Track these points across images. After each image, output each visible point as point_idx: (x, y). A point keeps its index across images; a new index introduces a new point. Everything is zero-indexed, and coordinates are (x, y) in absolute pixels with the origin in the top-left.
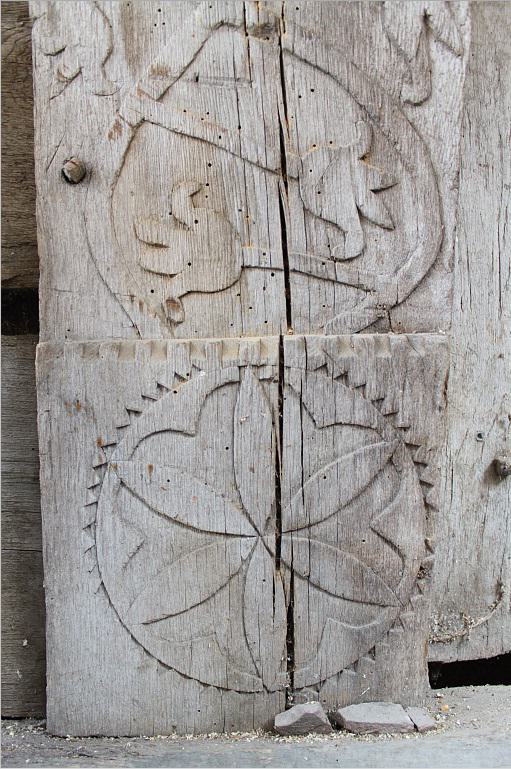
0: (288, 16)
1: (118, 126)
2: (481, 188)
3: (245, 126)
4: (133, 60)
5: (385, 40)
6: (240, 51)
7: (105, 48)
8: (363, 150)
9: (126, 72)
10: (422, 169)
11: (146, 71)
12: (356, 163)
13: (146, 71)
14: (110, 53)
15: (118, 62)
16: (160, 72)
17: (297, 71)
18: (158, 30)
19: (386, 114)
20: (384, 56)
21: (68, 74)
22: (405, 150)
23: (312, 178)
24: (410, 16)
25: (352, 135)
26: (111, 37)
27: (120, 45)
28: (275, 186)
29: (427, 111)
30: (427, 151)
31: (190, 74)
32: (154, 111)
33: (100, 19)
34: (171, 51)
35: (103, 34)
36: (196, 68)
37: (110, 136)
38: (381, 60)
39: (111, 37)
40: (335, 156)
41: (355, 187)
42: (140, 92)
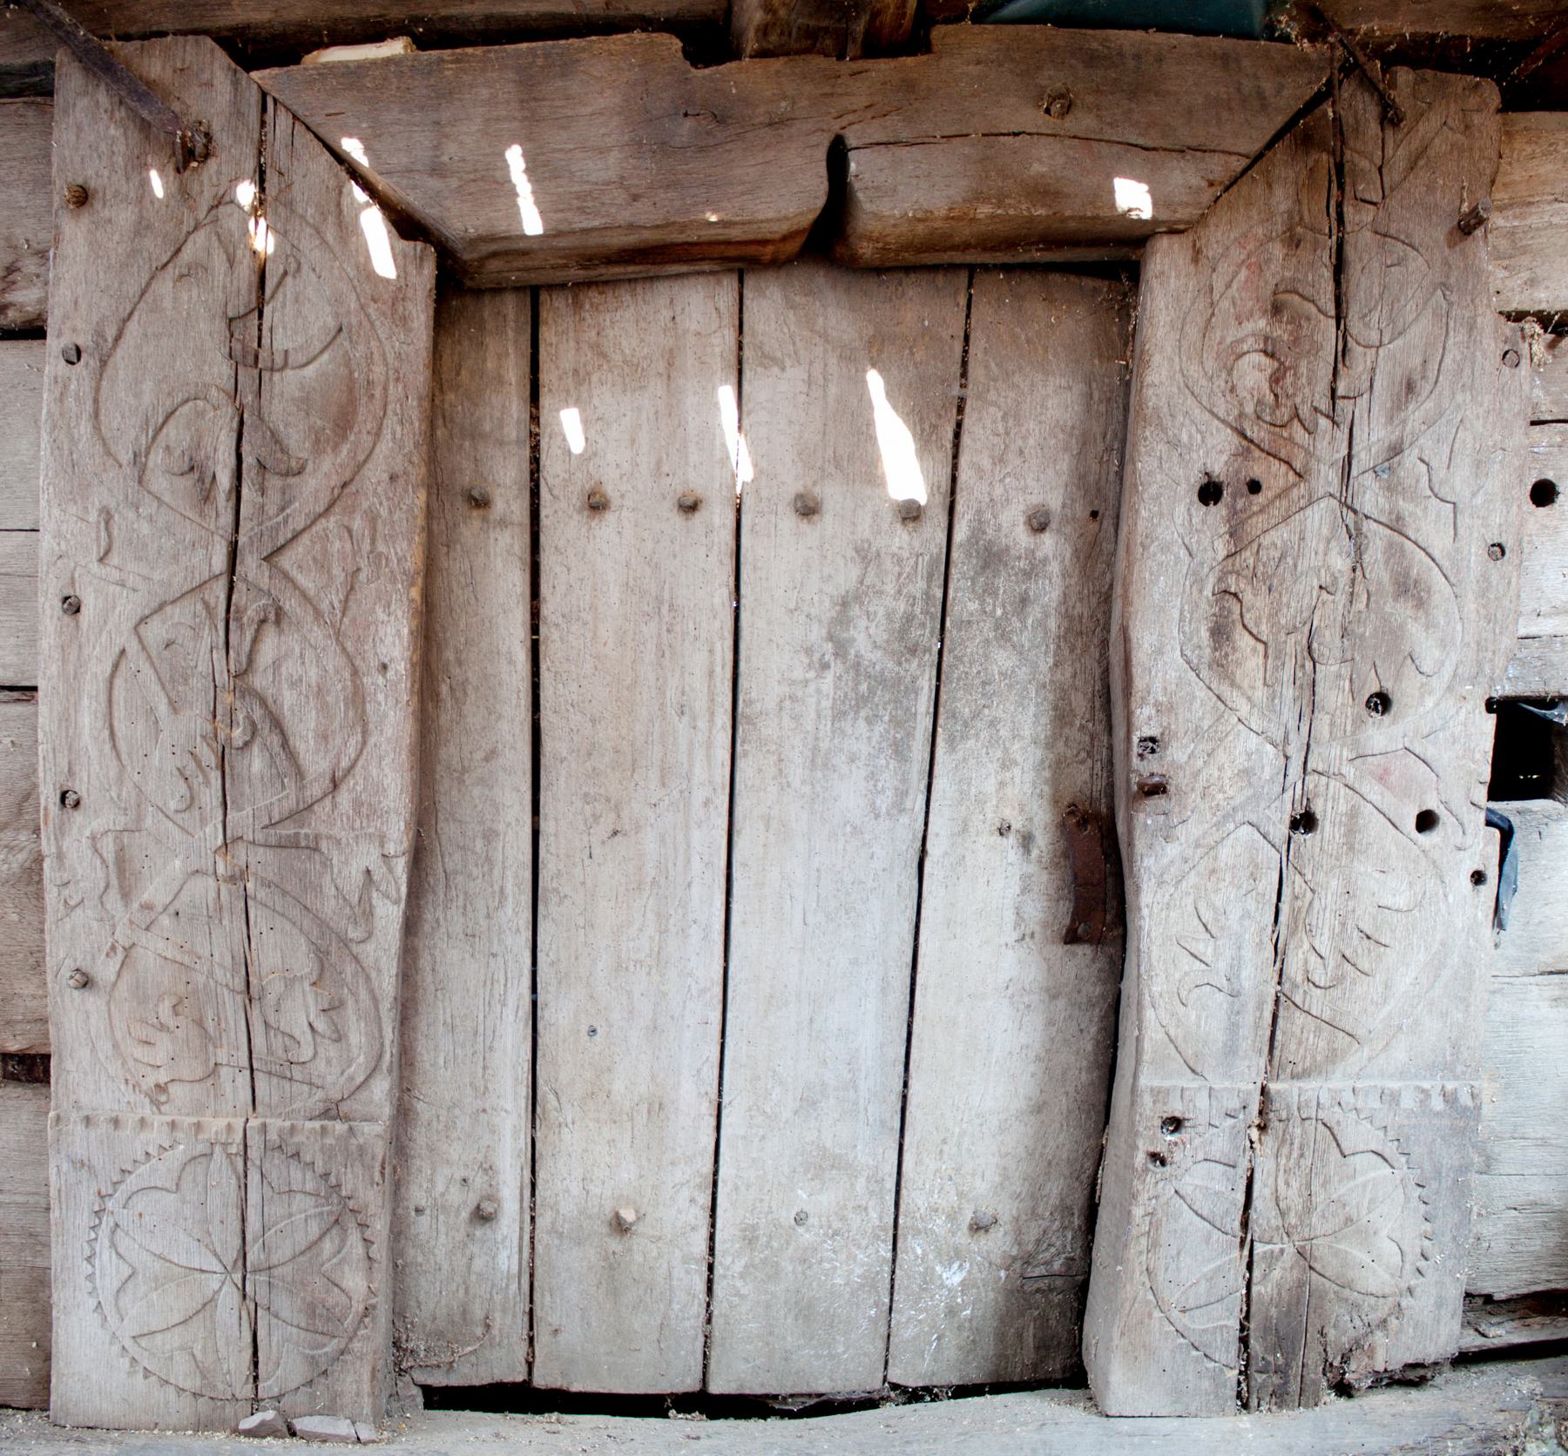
0: (252, 869)
1: (113, 948)
2: (467, 956)
3: (216, 956)
4: (126, 895)
5: (333, 889)
6: (212, 895)
7: (102, 885)
8: (314, 978)
9: (120, 905)
10: (363, 994)
11: (136, 905)
12: (308, 988)
13: (136, 905)
14: (107, 887)
15: (113, 896)
16: (148, 907)
17: (259, 913)
18: (146, 871)
19: (333, 949)
20: (333, 902)
21: (72, 903)
22: (349, 979)
23: (271, 999)
24: (354, 873)
25: (304, 964)
26: (108, 875)
27: (114, 882)
28: (241, 1004)
29: (369, 947)
30: (368, 978)
31: (171, 910)
32: (143, 938)
33: (98, 862)
34: (154, 891)
35: (101, 874)
36: (177, 905)
37: (107, 955)
38: (329, 906)
39: (108, 875)
40: (290, 983)
41: (307, 1007)
42: (131, 922)
